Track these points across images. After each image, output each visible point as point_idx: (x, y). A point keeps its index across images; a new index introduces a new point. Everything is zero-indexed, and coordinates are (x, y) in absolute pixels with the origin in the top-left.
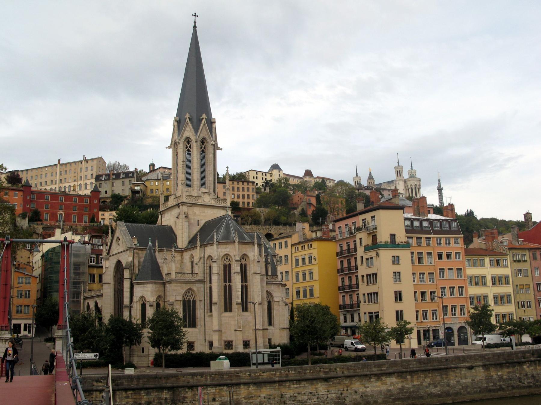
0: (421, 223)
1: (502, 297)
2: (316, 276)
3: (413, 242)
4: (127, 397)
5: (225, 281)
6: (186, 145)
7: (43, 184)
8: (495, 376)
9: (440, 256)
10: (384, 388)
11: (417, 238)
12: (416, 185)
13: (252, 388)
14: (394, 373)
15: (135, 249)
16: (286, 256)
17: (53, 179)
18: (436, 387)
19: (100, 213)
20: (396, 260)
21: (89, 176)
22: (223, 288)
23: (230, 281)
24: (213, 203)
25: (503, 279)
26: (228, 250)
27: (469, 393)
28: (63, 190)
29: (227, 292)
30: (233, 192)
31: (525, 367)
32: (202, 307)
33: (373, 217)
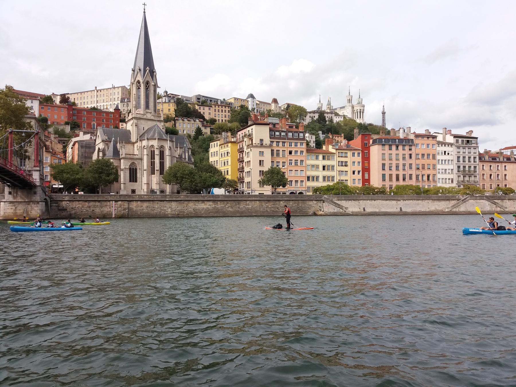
0: (280, 134)
1: (328, 177)
2: (230, 163)
3: (275, 144)
4: (79, 204)
5: (152, 159)
7: (86, 103)
8: (264, 206)
9: (290, 153)
10: (205, 207)
11: (277, 142)
12: (361, 110)
13: (139, 202)
14: (211, 200)
15: (106, 141)
16: (217, 152)
17: (92, 100)
18: (232, 208)
19: (121, 124)
20: (261, 153)
21: (116, 99)
23: (154, 159)
24: (152, 118)
25: (330, 167)
26: (153, 143)
27: (249, 212)
28: (99, 108)
29: (153, 164)
30: (215, 113)
31: (281, 202)
32: (141, 172)
33: (252, 129)
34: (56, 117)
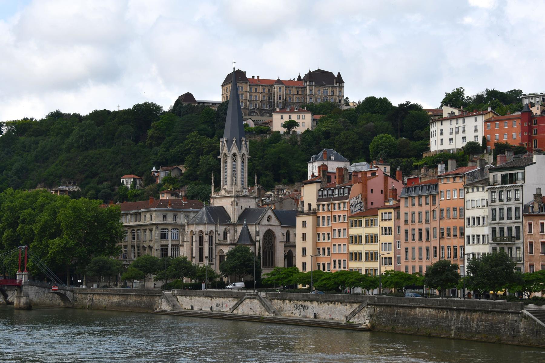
5: (200, 245)
22: (198, 248)
34: (506, 136)
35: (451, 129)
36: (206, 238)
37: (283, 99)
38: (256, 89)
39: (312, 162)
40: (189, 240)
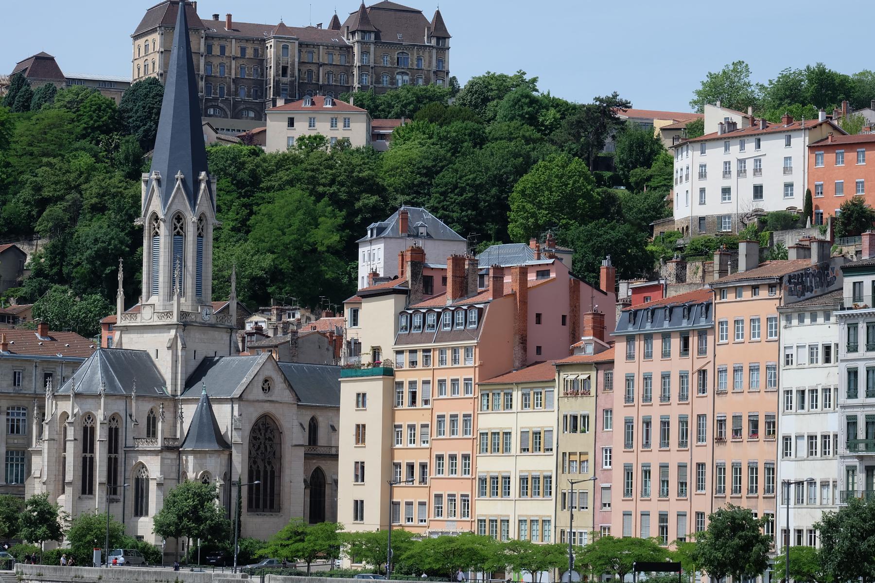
5: (85, 451)
6: (175, 225)
22: (81, 459)
35: (726, 163)
36: (100, 434)
37: (293, 75)
38: (223, 49)
39: (371, 242)
40: (56, 437)
